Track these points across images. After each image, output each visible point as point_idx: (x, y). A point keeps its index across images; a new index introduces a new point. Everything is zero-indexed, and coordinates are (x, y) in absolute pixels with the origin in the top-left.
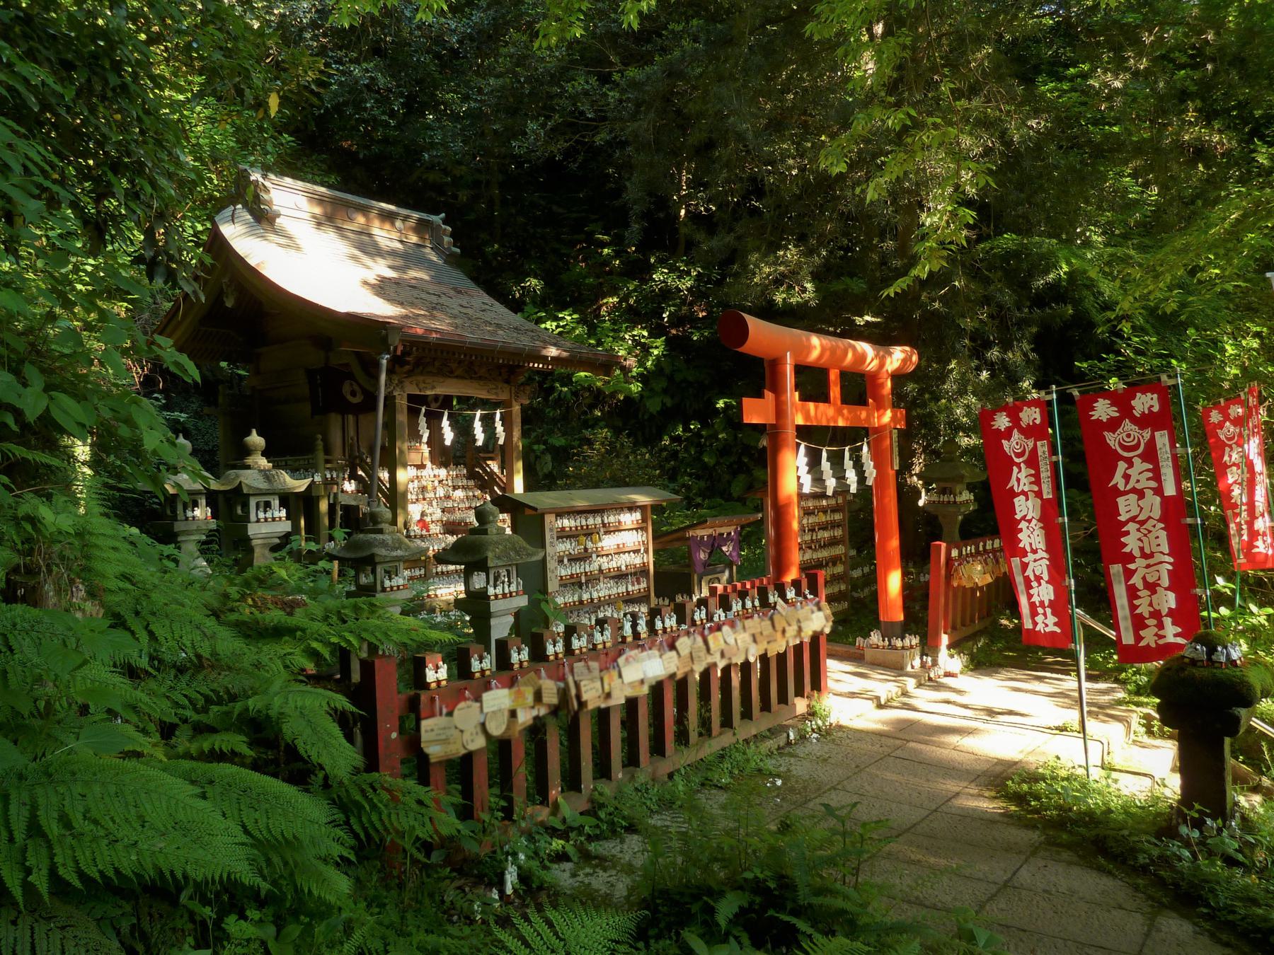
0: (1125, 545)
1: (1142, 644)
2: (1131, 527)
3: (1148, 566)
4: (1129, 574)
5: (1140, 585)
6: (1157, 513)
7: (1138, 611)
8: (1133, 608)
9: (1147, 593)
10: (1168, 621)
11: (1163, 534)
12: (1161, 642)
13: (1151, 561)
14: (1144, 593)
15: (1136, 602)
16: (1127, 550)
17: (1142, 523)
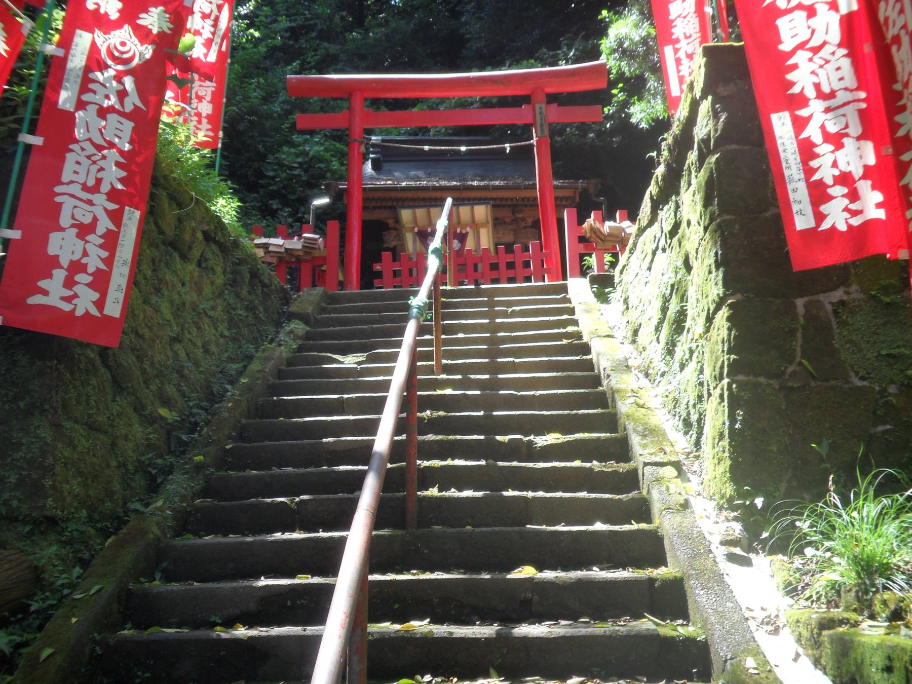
0: (792, 84)
1: (826, 225)
2: (801, 57)
4: (800, 124)
5: (817, 138)
6: (835, 36)
7: (816, 177)
8: (809, 172)
10: (864, 187)
11: (846, 63)
12: (856, 222)
14: (824, 149)
15: (814, 164)
16: (796, 90)
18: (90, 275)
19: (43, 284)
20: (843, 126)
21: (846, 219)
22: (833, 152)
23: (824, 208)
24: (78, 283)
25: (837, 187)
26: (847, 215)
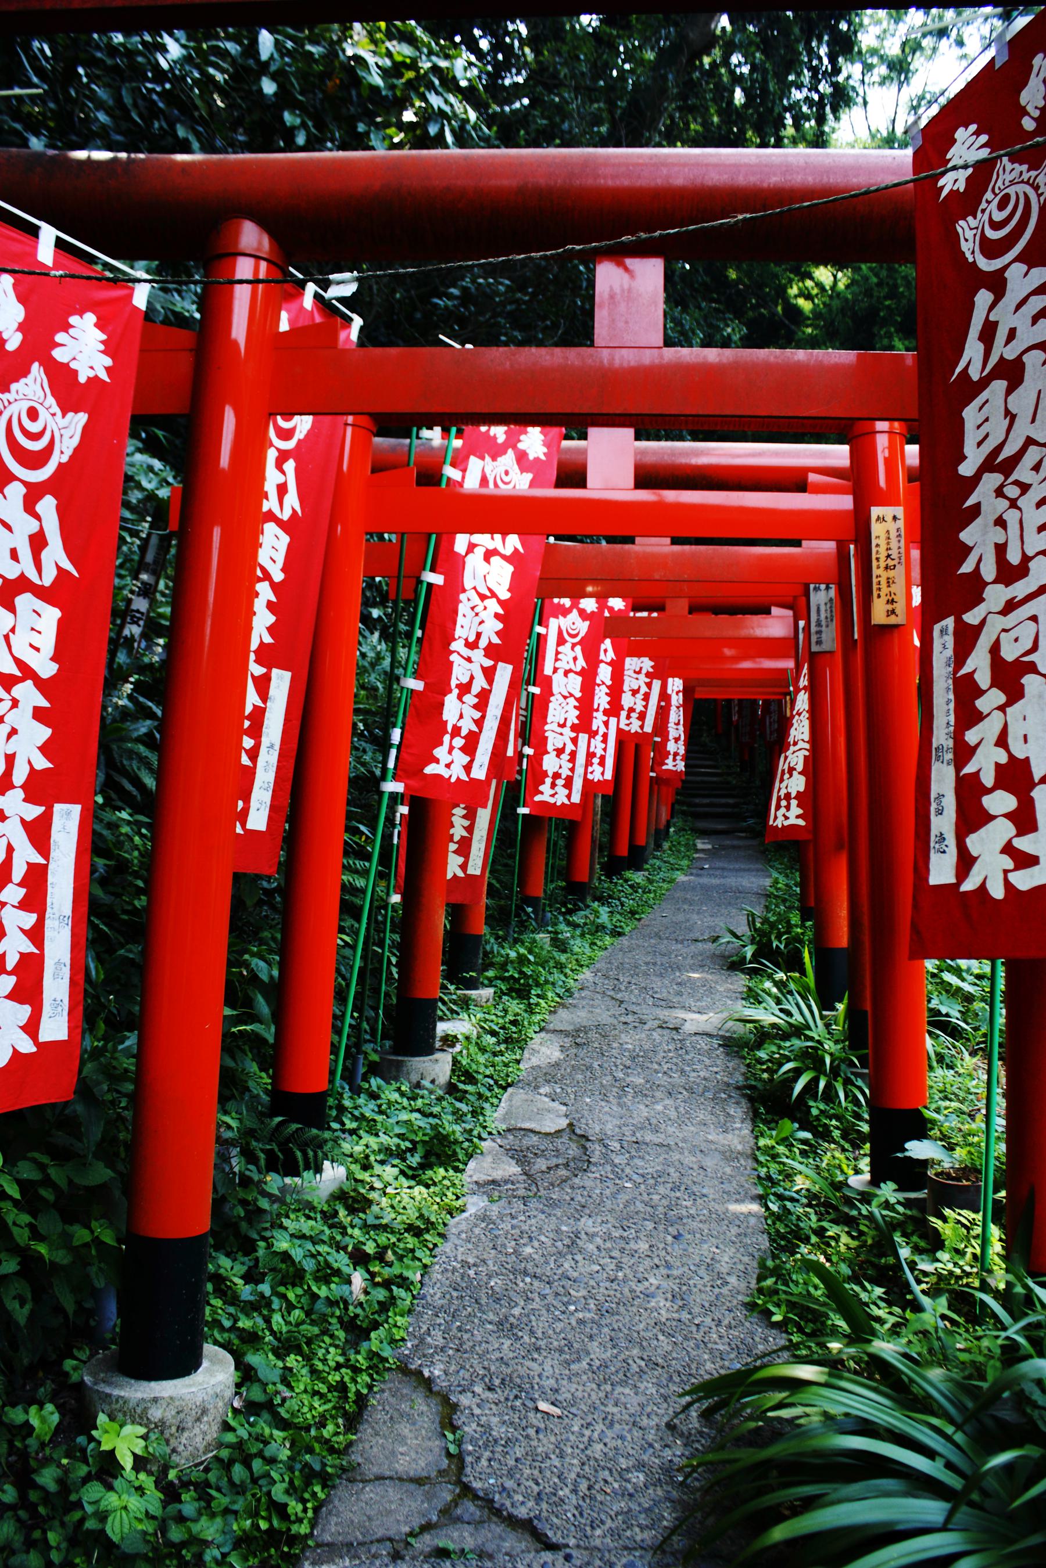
0: (967, 550)
3: (1010, 606)
5: (983, 679)
9: (996, 697)
13: (1020, 589)
14: (991, 700)
17: (1008, 467)
20: (1029, 645)
21: (1006, 872)
22: (1002, 708)
23: (973, 842)
25: (1000, 794)
26: (1008, 863)
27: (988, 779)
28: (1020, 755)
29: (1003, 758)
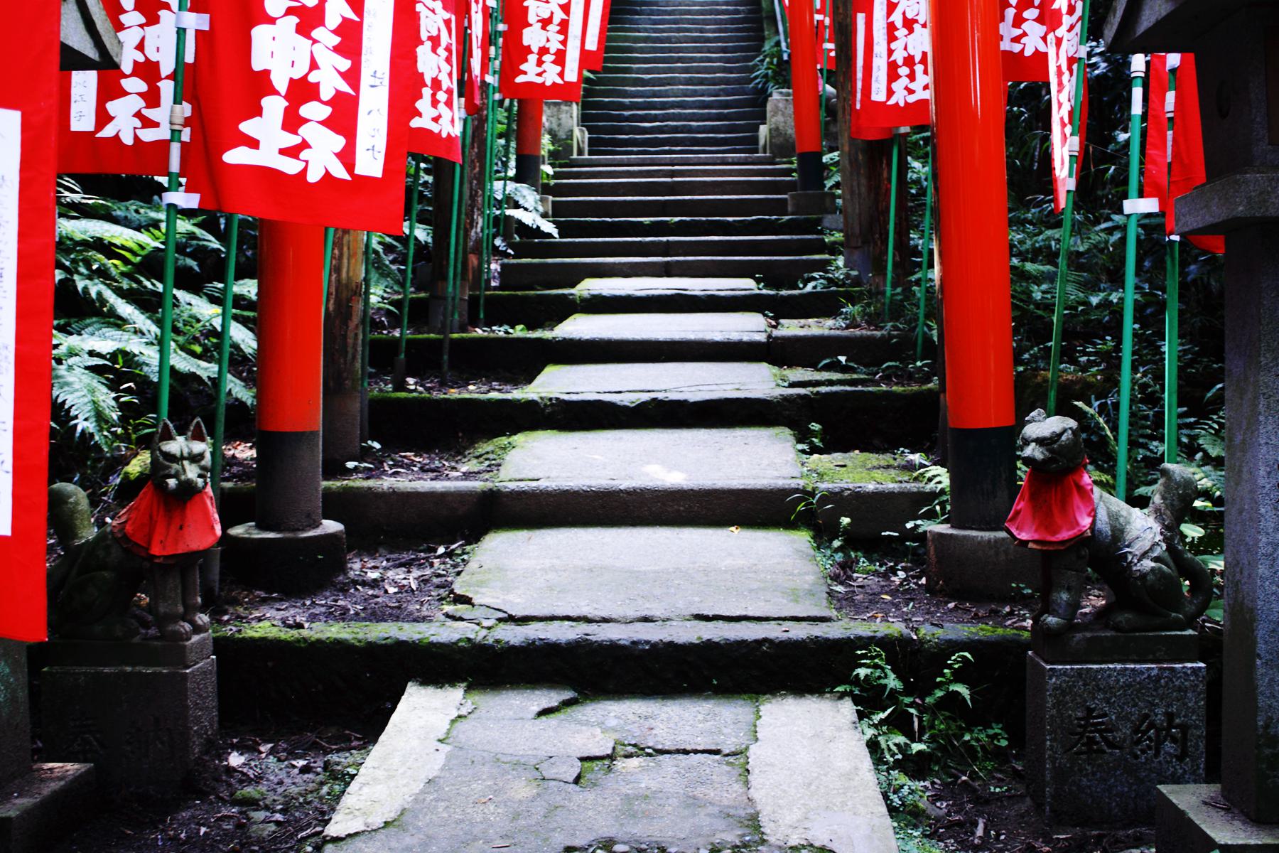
8: (890, 52)
18: (325, 103)
19: (247, 127)
24: (307, 121)
27: (900, 62)
28: (912, 54)
29: (906, 55)
